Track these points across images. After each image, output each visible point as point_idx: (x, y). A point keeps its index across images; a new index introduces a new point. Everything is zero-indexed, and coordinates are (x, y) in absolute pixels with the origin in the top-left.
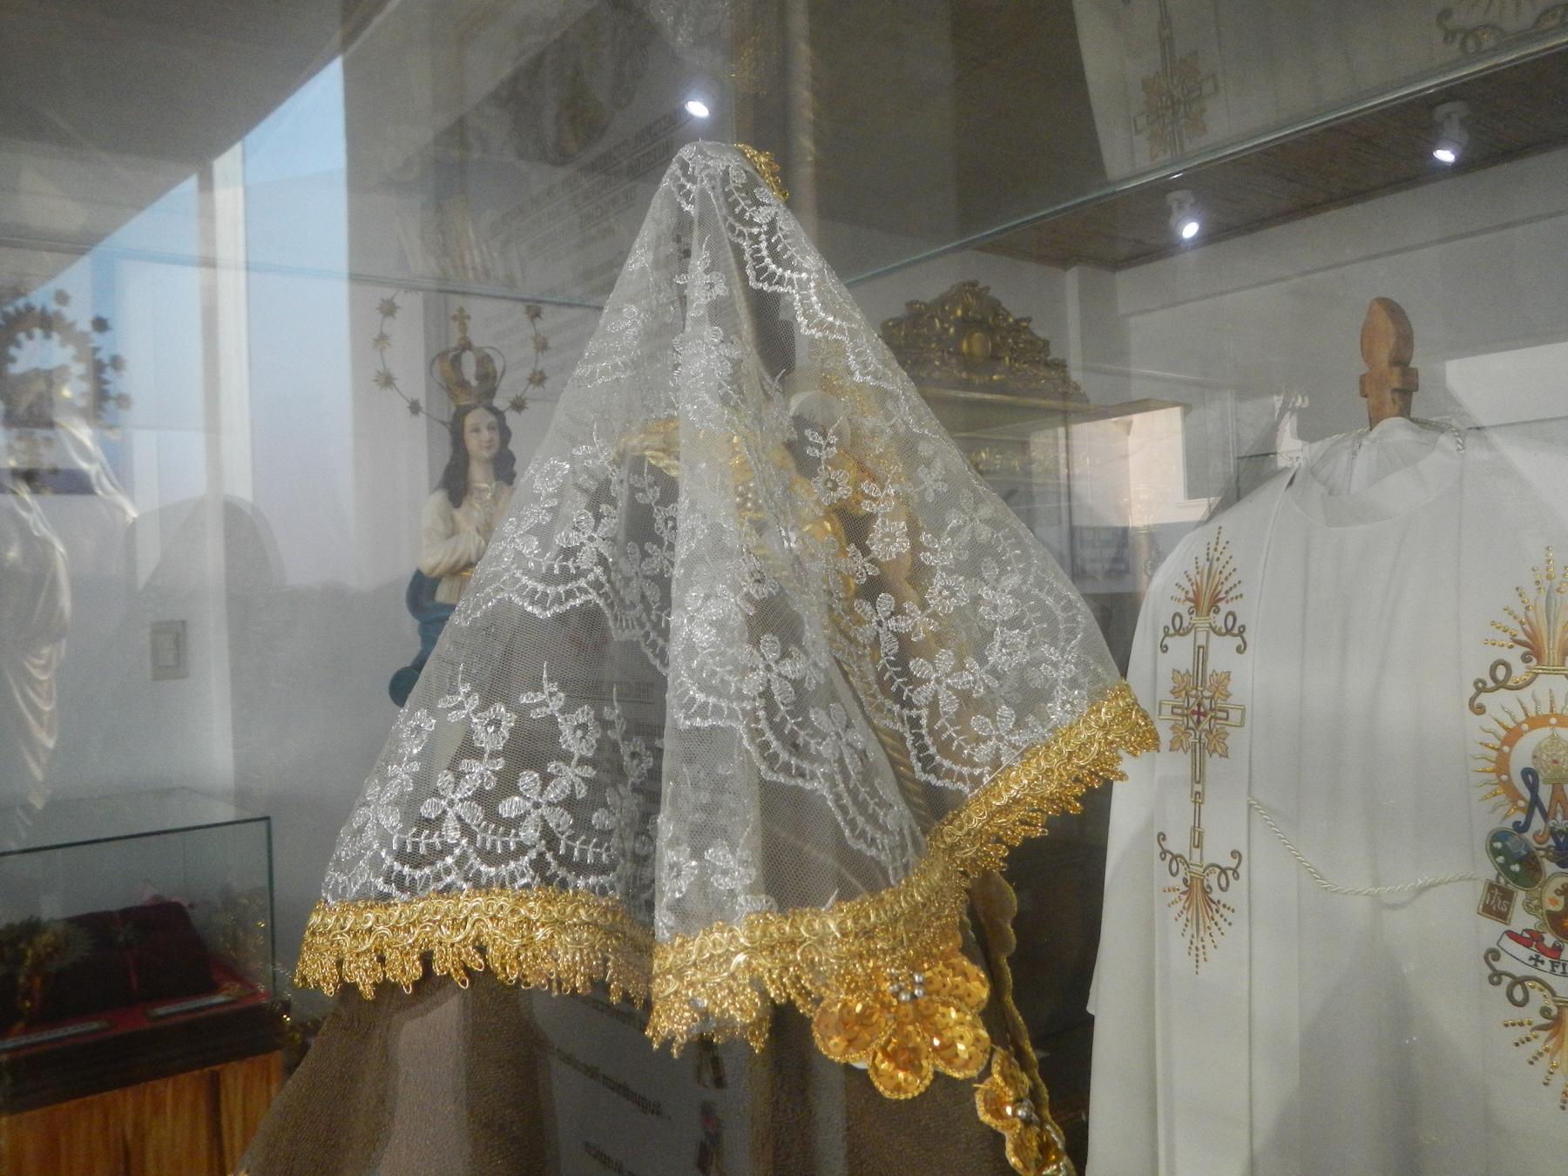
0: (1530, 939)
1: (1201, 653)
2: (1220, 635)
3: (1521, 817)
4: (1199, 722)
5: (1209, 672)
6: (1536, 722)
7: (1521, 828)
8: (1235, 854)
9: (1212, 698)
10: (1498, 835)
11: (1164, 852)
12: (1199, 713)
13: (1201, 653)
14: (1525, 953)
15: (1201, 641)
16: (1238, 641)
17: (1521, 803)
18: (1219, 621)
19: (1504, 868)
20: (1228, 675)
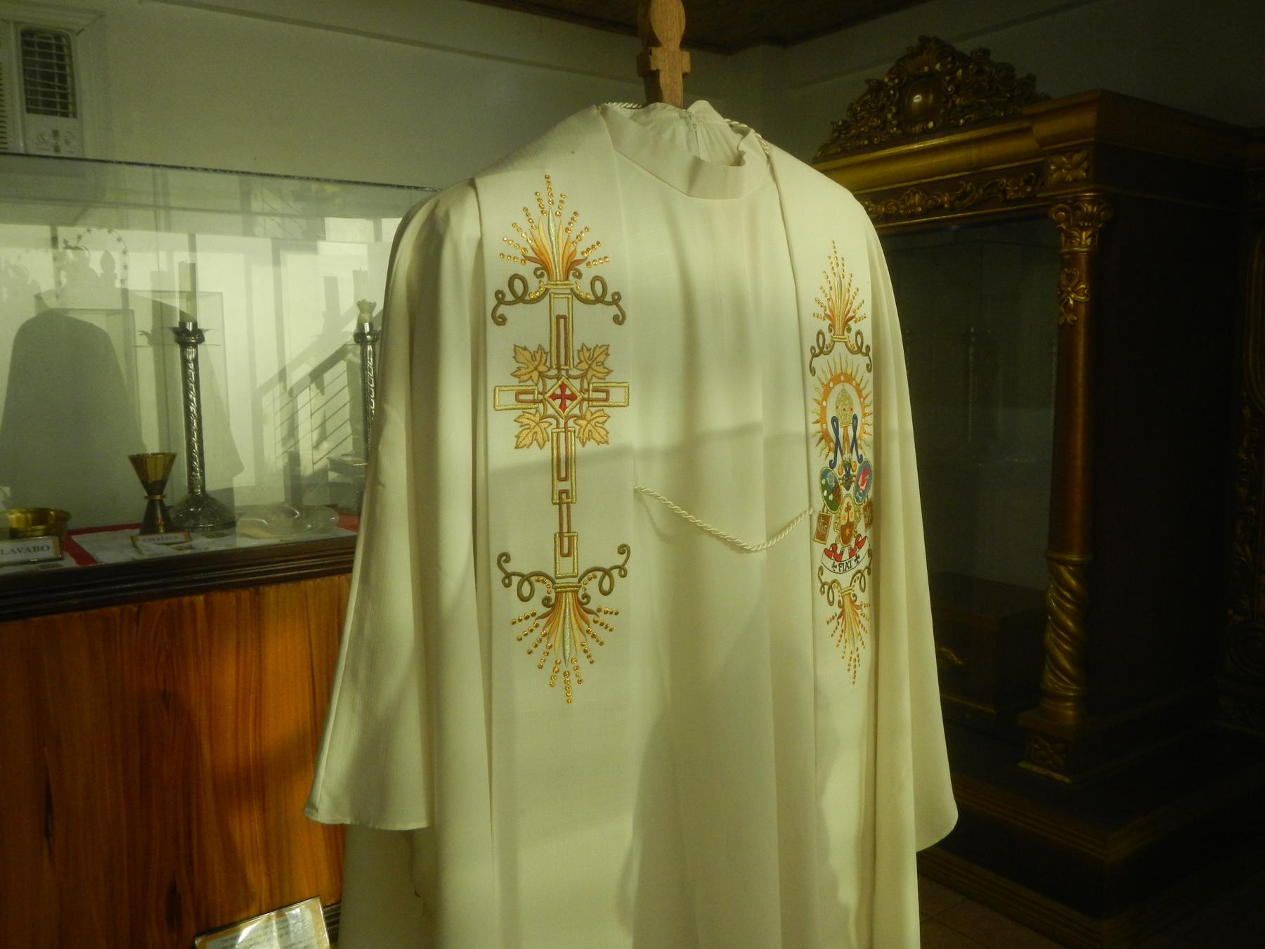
0: (832, 553)
1: (562, 323)
2: (585, 301)
3: (831, 456)
4: (563, 407)
5: (577, 346)
6: (836, 379)
7: (833, 464)
8: (623, 549)
9: (582, 377)
10: (824, 474)
11: (508, 576)
12: (563, 397)
13: (562, 323)
14: (829, 562)
15: (561, 307)
16: (613, 310)
17: (832, 445)
18: (583, 287)
19: (826, 498)
20: (606, 350)
